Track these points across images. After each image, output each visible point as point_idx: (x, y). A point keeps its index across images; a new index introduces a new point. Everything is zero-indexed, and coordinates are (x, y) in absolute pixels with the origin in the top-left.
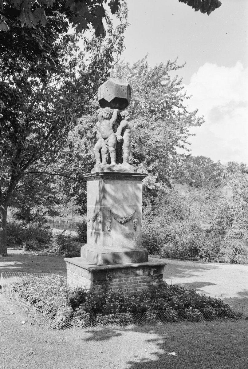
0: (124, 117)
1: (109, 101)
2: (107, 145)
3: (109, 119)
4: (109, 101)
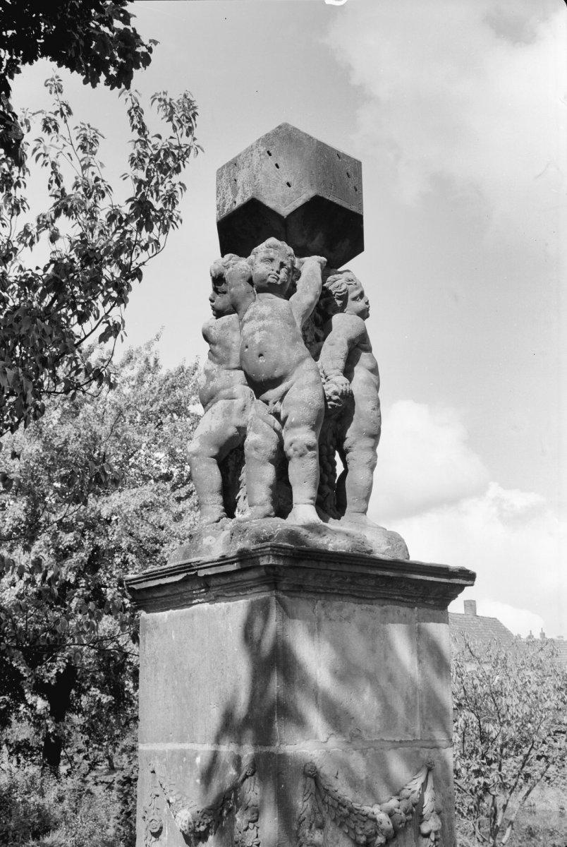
0: (344, 298)
1: (285, 211)
2: (277, 415)
3: (287, 290)
4: (285, 211)
